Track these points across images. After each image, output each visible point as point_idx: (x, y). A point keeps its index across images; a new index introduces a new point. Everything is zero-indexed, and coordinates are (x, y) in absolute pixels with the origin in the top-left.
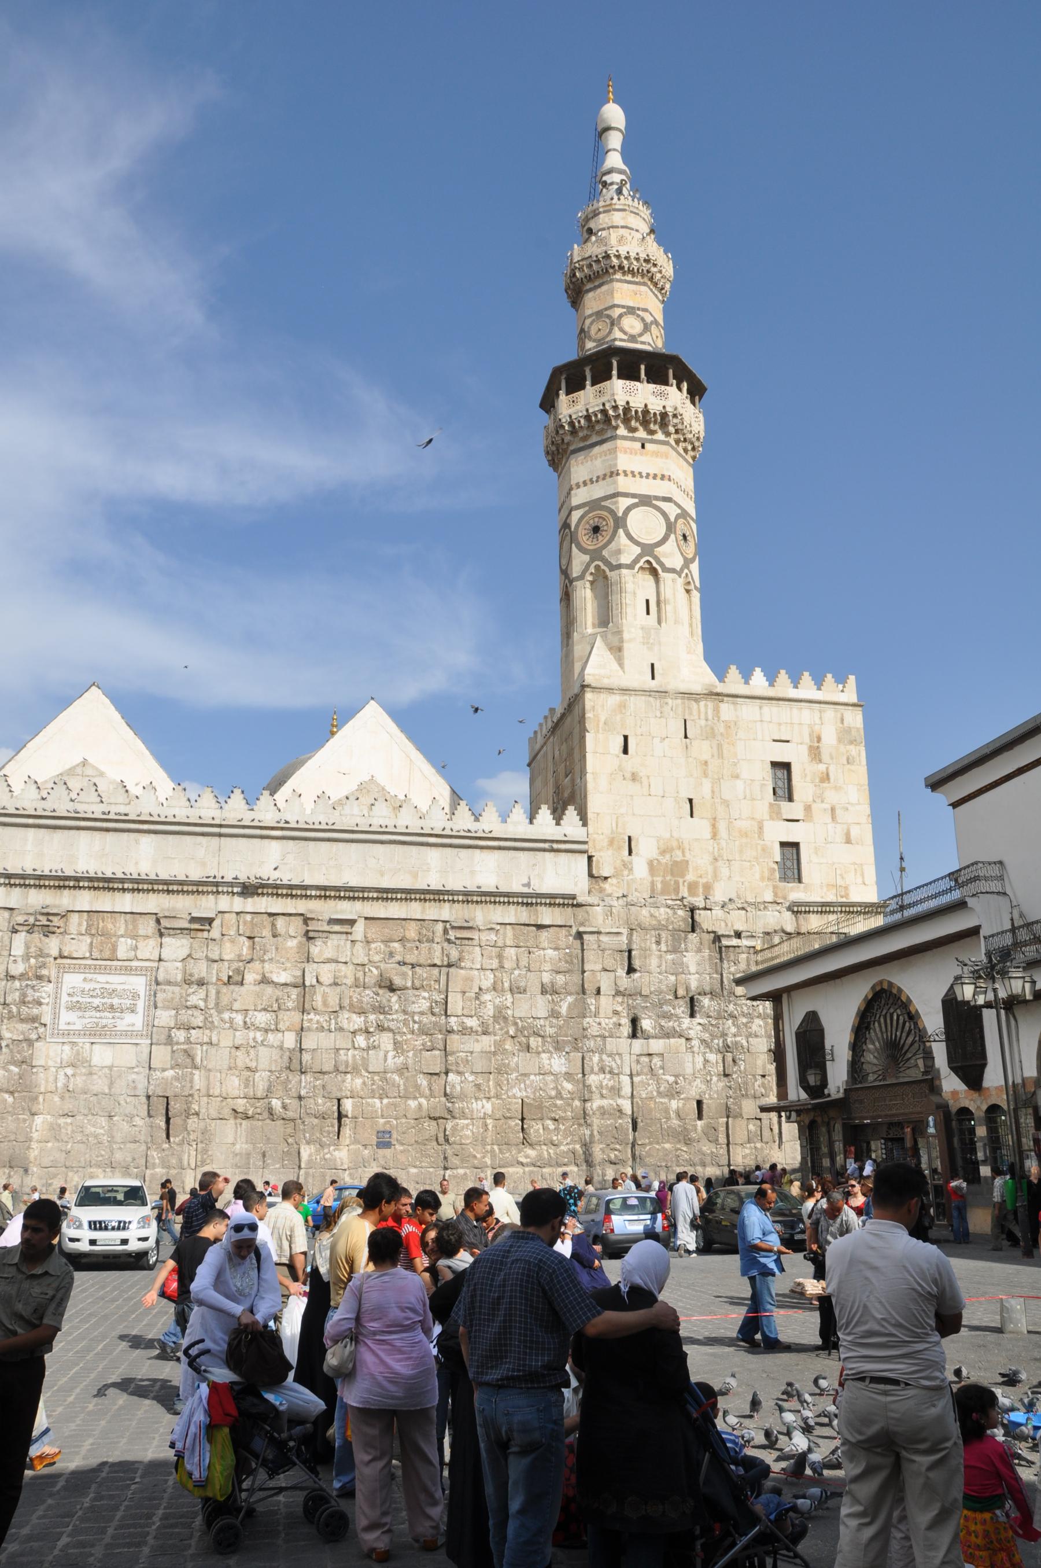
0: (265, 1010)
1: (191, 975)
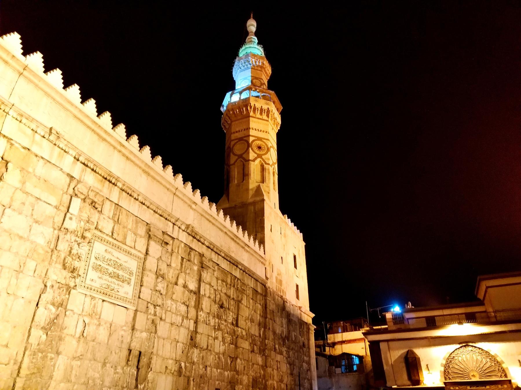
0: (184, 303)
1: (160, 270)
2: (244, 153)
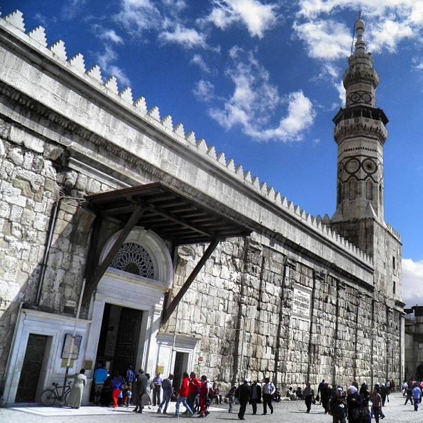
2: (356, 172)
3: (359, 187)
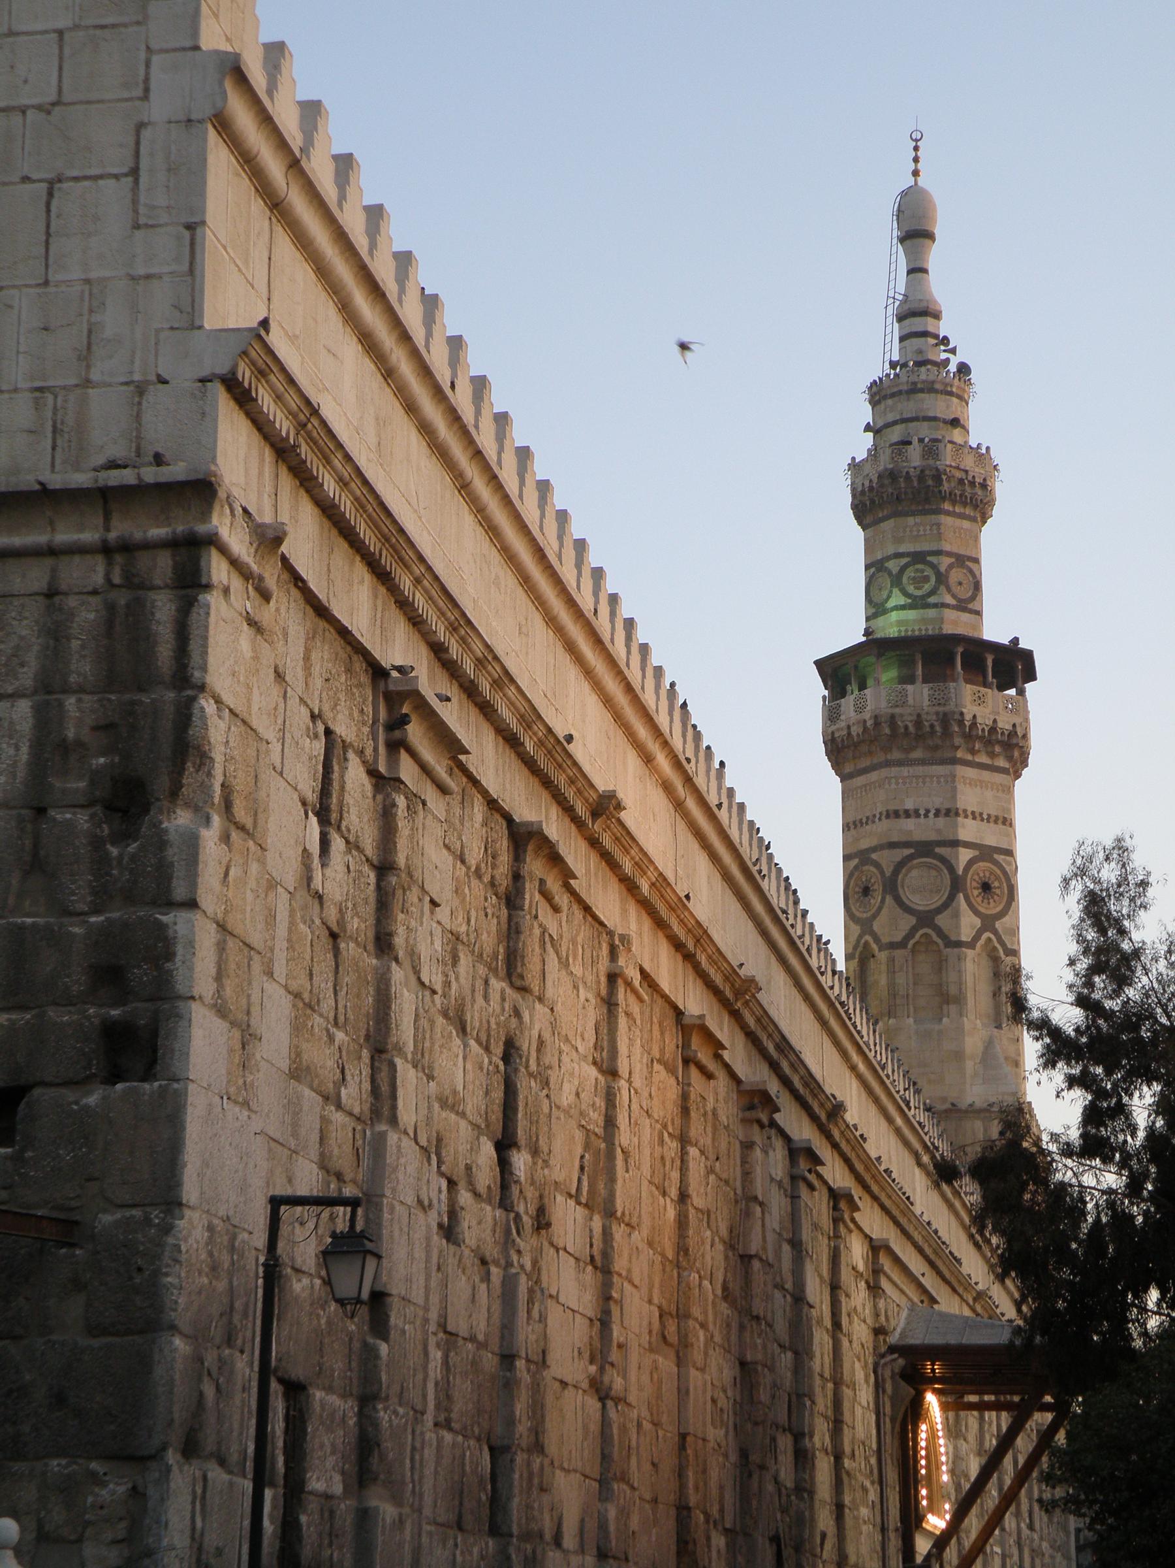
3: (952, 977)
